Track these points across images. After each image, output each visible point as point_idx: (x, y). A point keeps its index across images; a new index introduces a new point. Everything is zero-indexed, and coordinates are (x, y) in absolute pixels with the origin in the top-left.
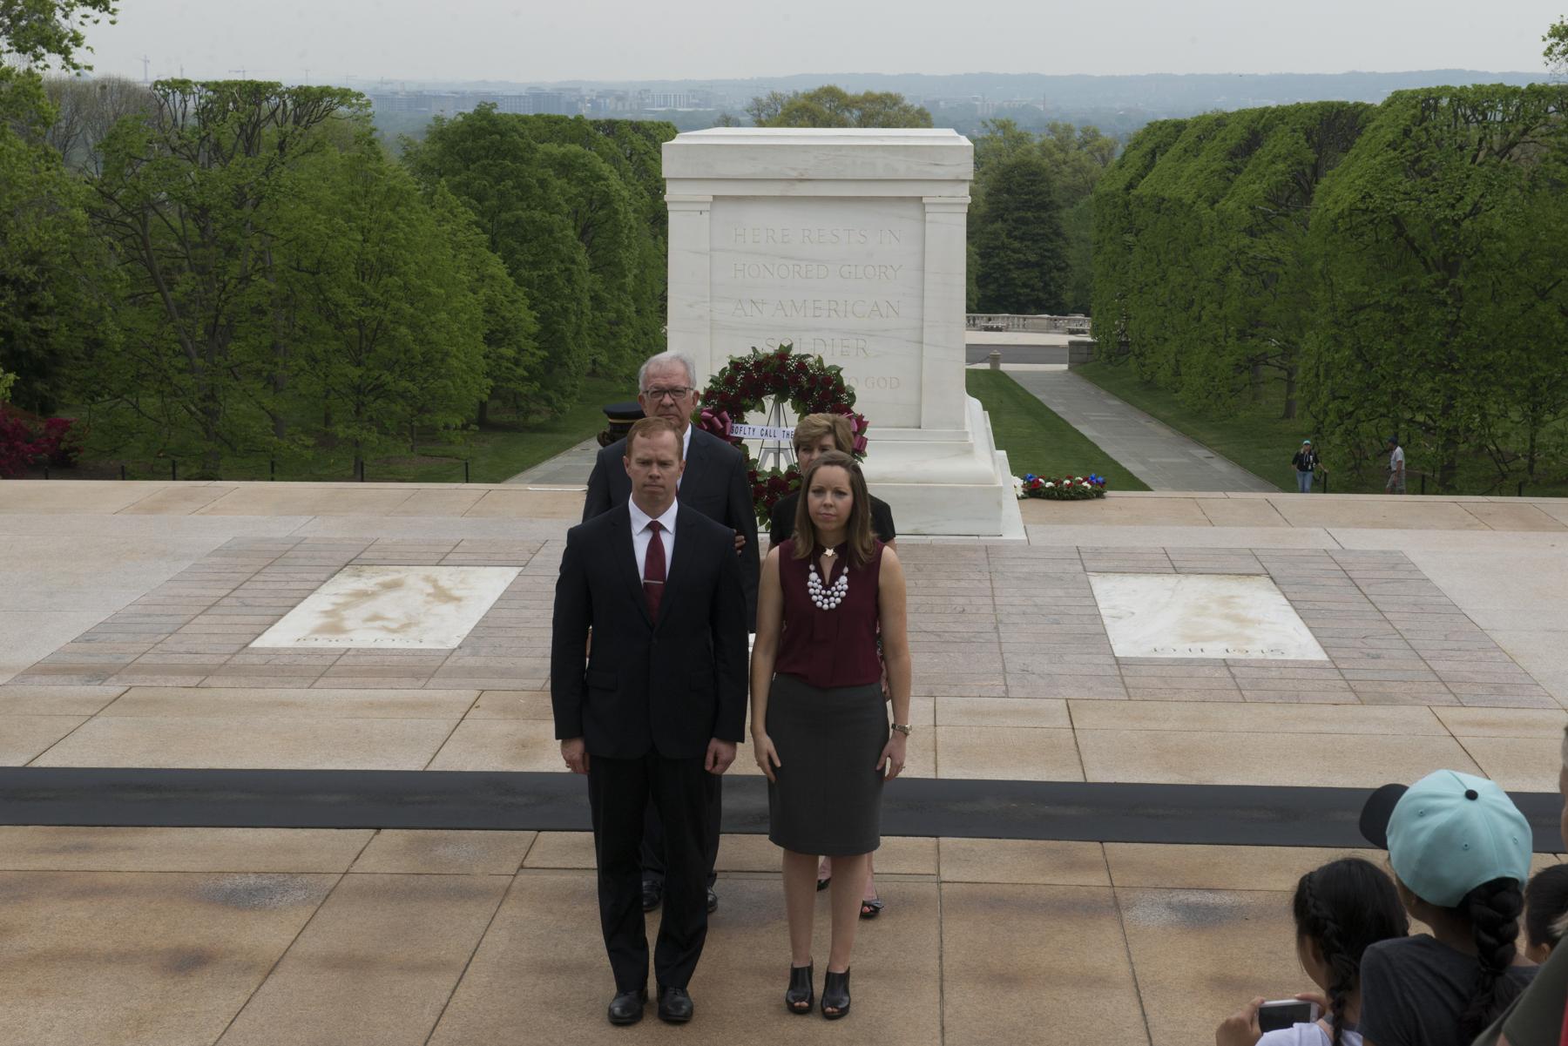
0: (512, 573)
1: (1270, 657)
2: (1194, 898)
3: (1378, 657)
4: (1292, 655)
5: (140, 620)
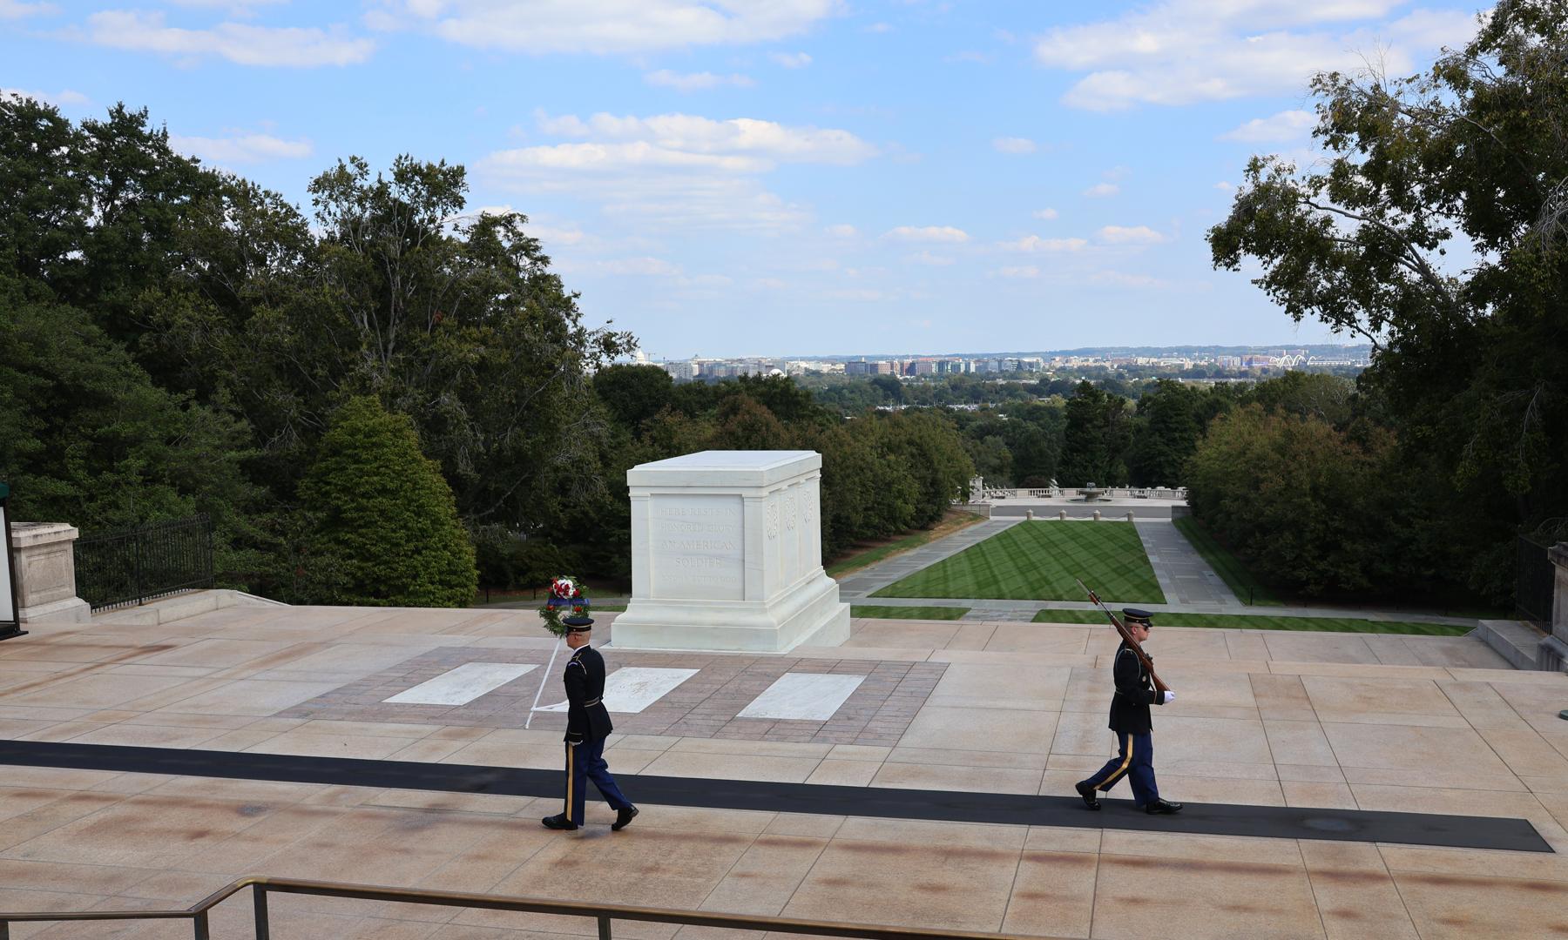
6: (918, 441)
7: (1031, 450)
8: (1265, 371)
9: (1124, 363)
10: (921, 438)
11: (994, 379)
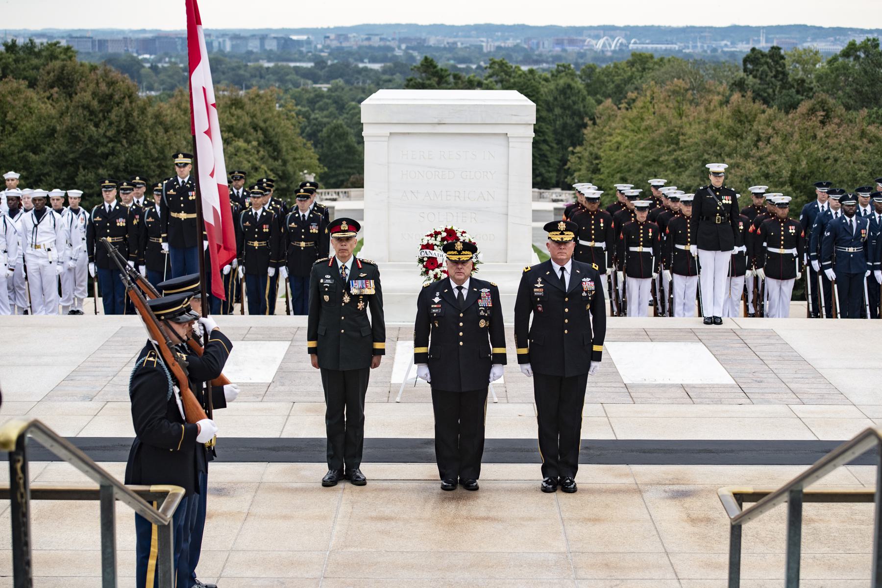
0: (287, 344)
1: (705, 382)
2: (676, 487)
3: (761, 382)
4: (717, 381)
5: (94, 369)
6: (262, 124)
7: (336, 145)
8: (582, 55)
9: (414, 43)
10: (265, 121)
11: (257, 60)
